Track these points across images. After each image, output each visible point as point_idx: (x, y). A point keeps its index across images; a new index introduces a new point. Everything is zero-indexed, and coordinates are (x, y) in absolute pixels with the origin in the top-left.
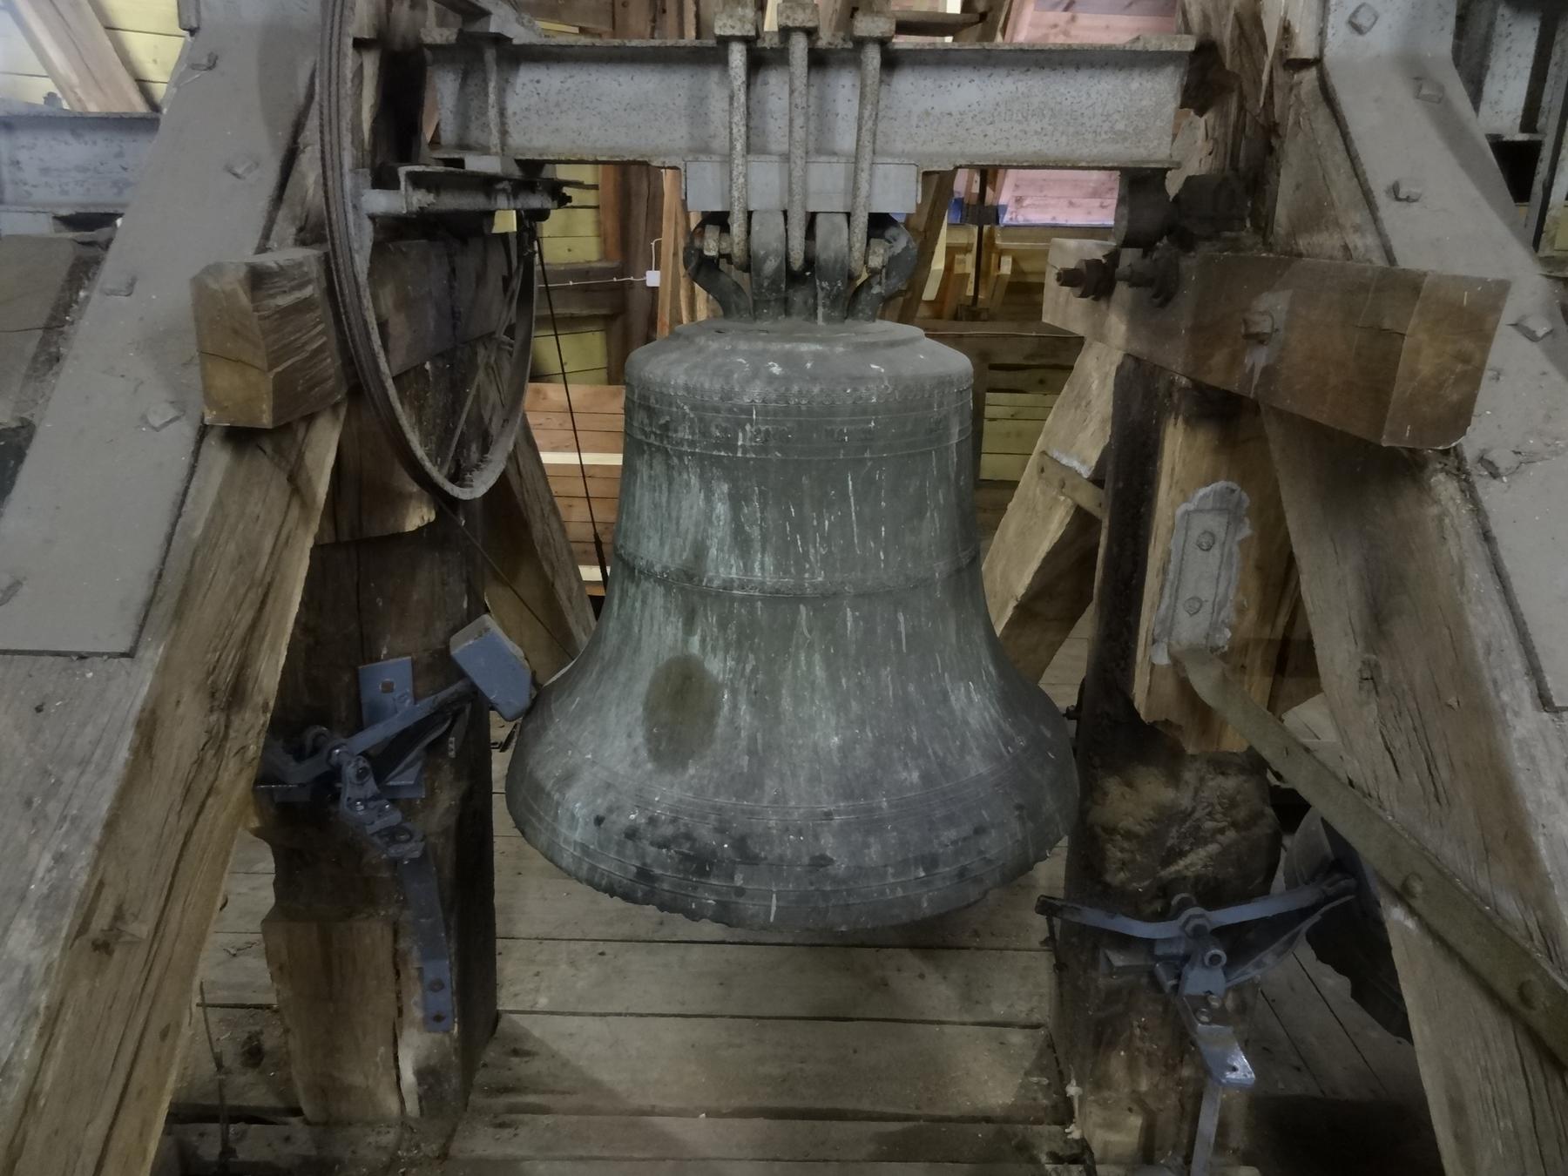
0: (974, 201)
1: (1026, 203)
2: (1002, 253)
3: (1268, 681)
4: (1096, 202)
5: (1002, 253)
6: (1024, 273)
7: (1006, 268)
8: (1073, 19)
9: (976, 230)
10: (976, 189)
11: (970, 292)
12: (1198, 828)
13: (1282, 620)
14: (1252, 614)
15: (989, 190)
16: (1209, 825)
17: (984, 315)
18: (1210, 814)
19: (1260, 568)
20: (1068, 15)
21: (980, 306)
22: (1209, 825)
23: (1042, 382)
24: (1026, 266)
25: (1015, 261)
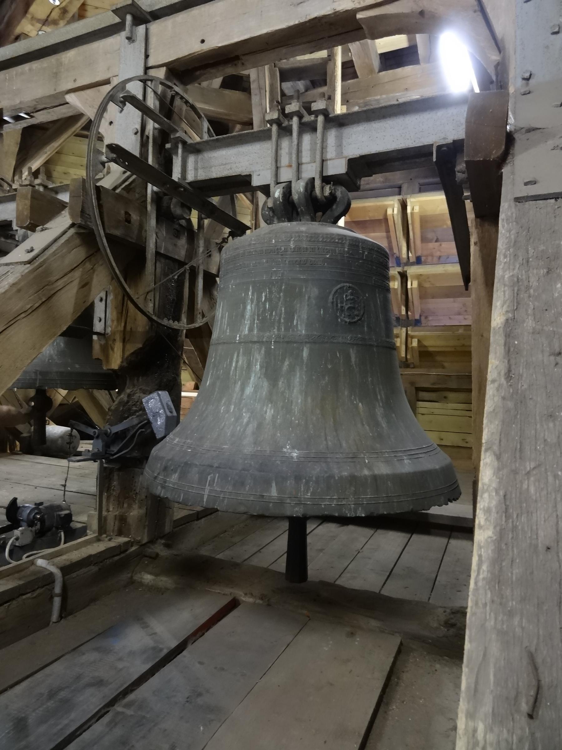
0: (404, 318)
1: (430, 318)
2: (412, 337)
3: (121, 344)
4: (461, 317)
5: (412, 337)
6: (425, 346)
7: (415, 343)
8: (441, 245)
9: (404, 330)
10: (404, 312)
11: (403, 354)
12: (130, 409)
13: (123, 324)
14: (115, 323)
15: (409, 313)
16: (134, 408)
17: (412, 366)
18: (134, 405)
19: (116, 308)
20: (438, 244)
21: (409, 362)
22: (134, 408)
23: (445, 397)
24: (426, 343)
25: (419, 341)
